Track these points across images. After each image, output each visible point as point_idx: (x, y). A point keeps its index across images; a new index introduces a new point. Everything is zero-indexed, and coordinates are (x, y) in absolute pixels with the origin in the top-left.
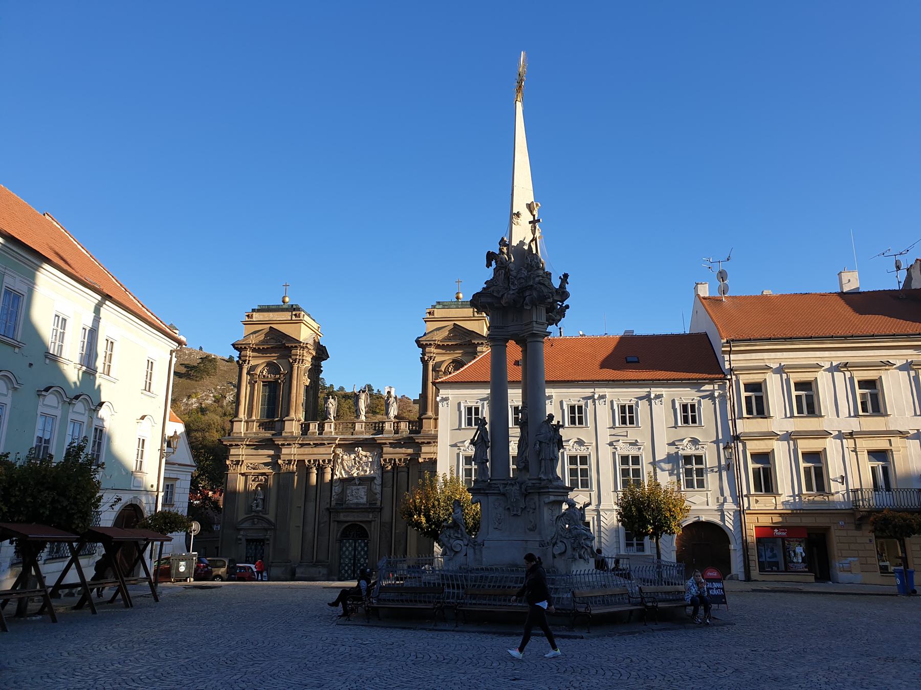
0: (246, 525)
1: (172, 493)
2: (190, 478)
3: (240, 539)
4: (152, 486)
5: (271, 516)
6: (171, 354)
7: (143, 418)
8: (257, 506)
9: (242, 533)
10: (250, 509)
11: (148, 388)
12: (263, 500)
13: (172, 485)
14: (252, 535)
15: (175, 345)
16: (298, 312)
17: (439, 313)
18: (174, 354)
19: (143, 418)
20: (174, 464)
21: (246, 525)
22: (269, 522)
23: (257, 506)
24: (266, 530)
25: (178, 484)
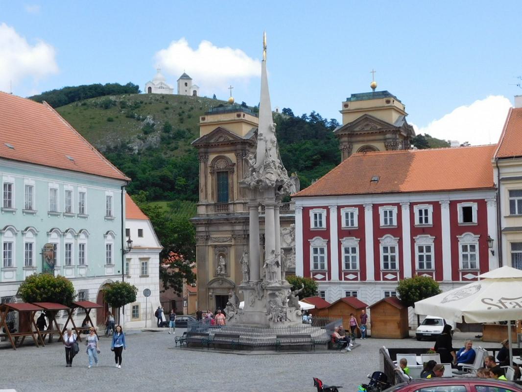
0: (215, 285)
1: (146, 268)
2: (158, 256)
3: (211, 296)
4: (119, 272)
5: (232, 278)
6: (122, 189)
7: (107, 233)
8: (221, 270)
9: (212, 291)
10: (216, 274)
11: (109, 213)
12: (225, 266)
13: (146, 263)
14: (220, 293)
15: (123, 183)
16: (238, 113)
17: (353, 106)
18: (124, 188)
19: (107, 233)
20: (145, 248)
21: (215, 285)
22: (230, 283)
23: (221, 270)
24: (229, 289)
25: (150, 262)
